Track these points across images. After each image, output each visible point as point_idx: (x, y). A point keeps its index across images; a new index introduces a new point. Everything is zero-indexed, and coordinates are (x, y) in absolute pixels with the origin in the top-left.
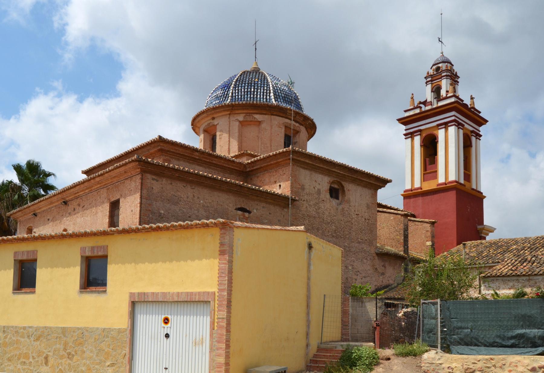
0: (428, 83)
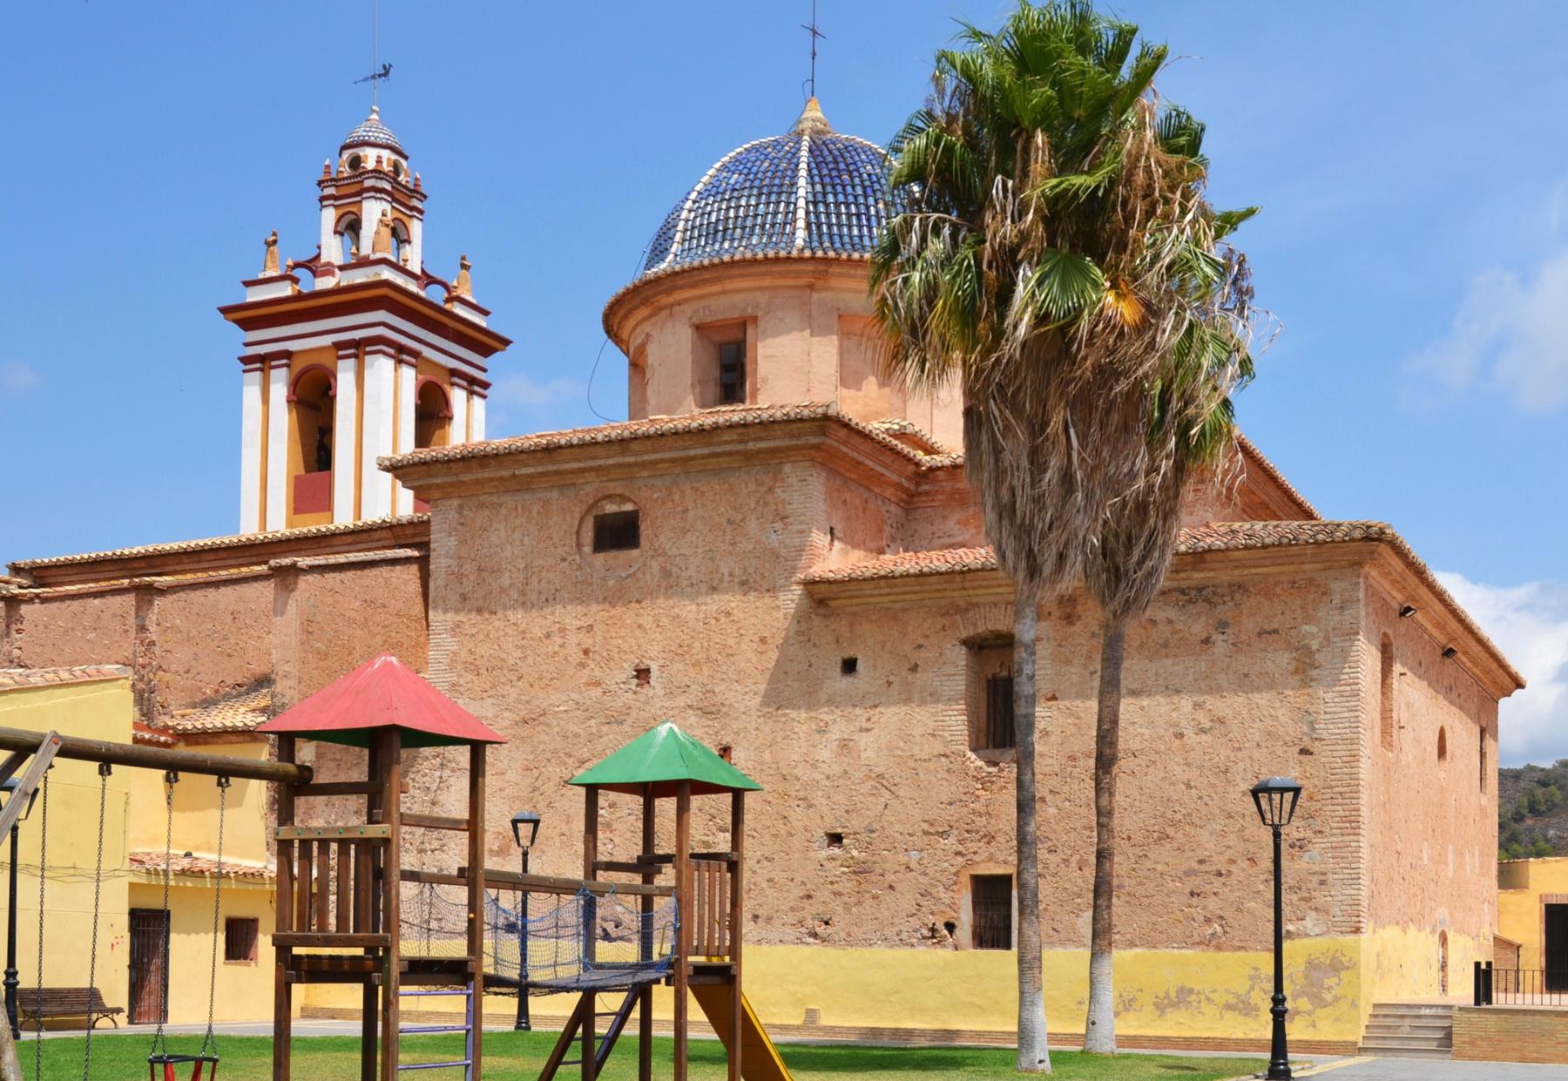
0: (325, 203)
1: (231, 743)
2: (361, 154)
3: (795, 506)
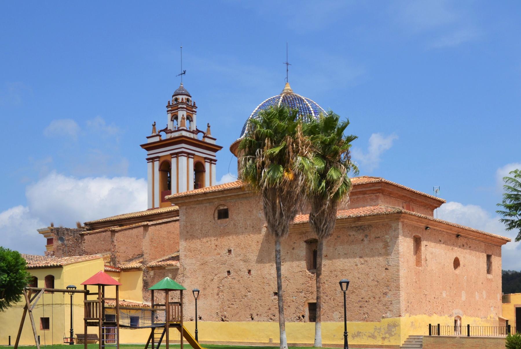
0: (168, 112)
1: (134, 271)
2: (178, 98)
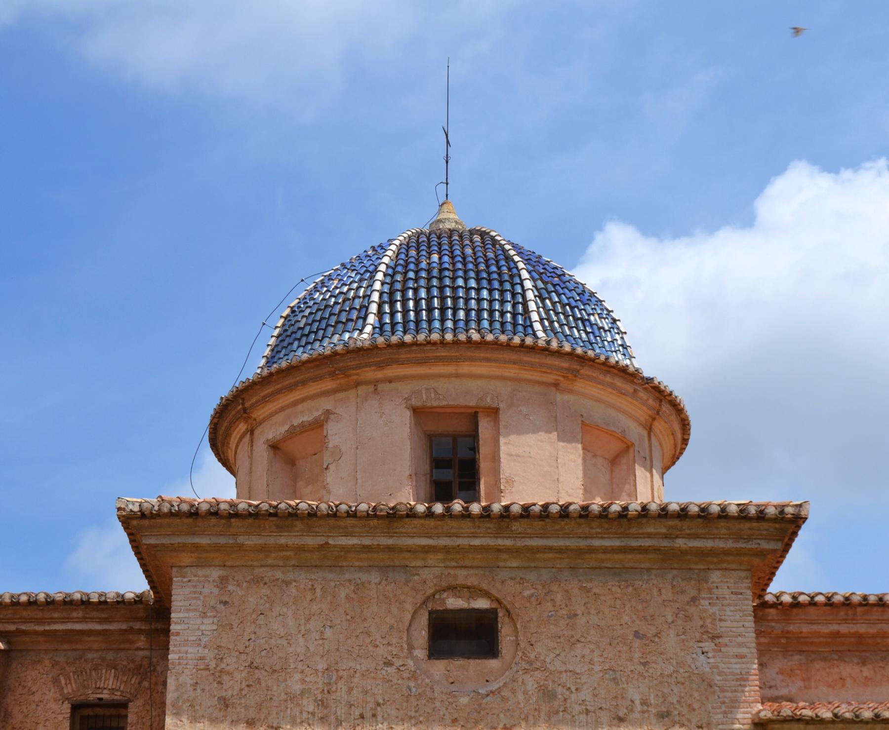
3: (728, 624)
